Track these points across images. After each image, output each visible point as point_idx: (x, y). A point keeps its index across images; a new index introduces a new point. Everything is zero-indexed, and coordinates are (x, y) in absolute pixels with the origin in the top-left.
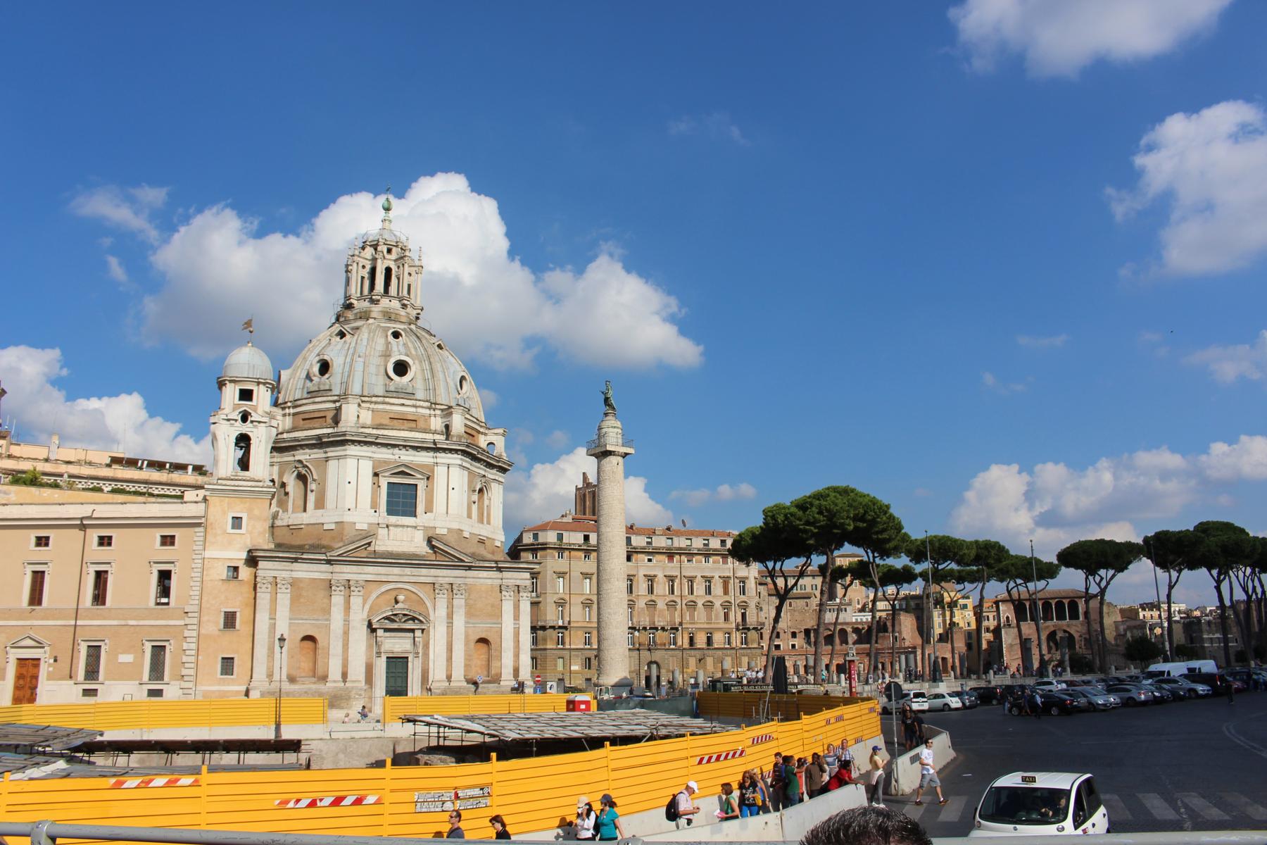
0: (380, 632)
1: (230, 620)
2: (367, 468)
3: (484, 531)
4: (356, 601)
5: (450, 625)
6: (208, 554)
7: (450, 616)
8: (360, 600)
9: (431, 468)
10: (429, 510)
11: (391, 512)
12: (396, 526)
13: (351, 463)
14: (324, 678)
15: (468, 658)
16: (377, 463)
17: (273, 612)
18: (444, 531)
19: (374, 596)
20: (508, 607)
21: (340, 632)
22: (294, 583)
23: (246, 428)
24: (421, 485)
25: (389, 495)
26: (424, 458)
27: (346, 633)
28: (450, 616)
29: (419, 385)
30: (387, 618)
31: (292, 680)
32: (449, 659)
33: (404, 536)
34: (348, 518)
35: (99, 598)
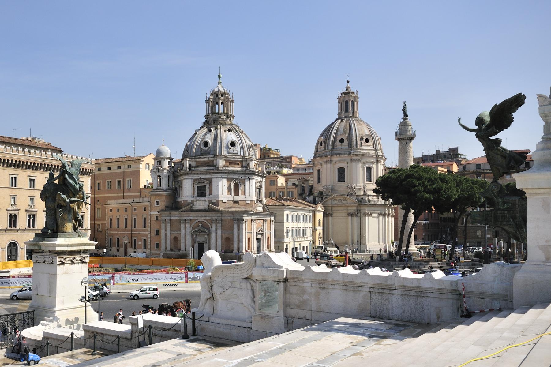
0: (195, 236)
1: (157, 231)
2: (190, 182)
3: (240, 197)
4: (188, 226)
5: (216, 233)
6: (152, 213)
7: (216, 230)
8: (189, 225)
9: (210, 180)
10: (210, 194)
11: (199, 195)
12: (199, 200)
13: (186, 181)
14: (180, 250)
15: (222, 244)
16: (194, 180)
17: (166, 230)
18: (214, 201)
19: (193, 224)
20: (235, 227)
21: (184, 236)
22: (171, 220)
23: (159, 174)
24: (207, 186)
25: (198, 190)
26: (208, 176)
27: (185, 236)
28: (216, 230)
29: (212, 149)
30: (196, 231)
31: (171, 250)
32: (216, 244)
33: (201, 204)
34: (186, 199)
35: (135, 227)
